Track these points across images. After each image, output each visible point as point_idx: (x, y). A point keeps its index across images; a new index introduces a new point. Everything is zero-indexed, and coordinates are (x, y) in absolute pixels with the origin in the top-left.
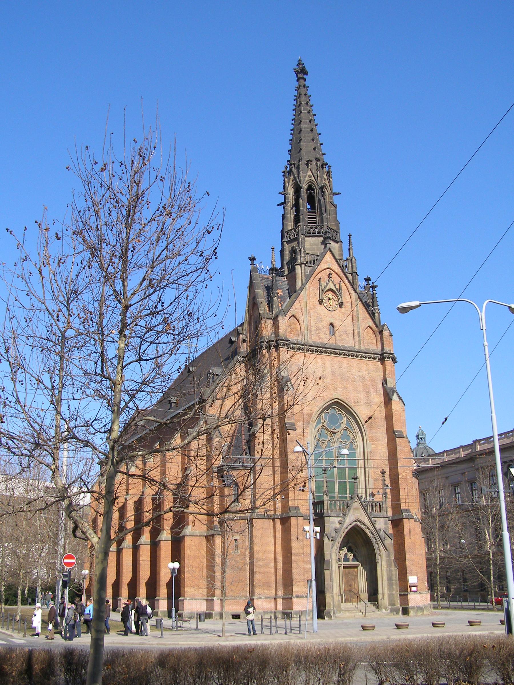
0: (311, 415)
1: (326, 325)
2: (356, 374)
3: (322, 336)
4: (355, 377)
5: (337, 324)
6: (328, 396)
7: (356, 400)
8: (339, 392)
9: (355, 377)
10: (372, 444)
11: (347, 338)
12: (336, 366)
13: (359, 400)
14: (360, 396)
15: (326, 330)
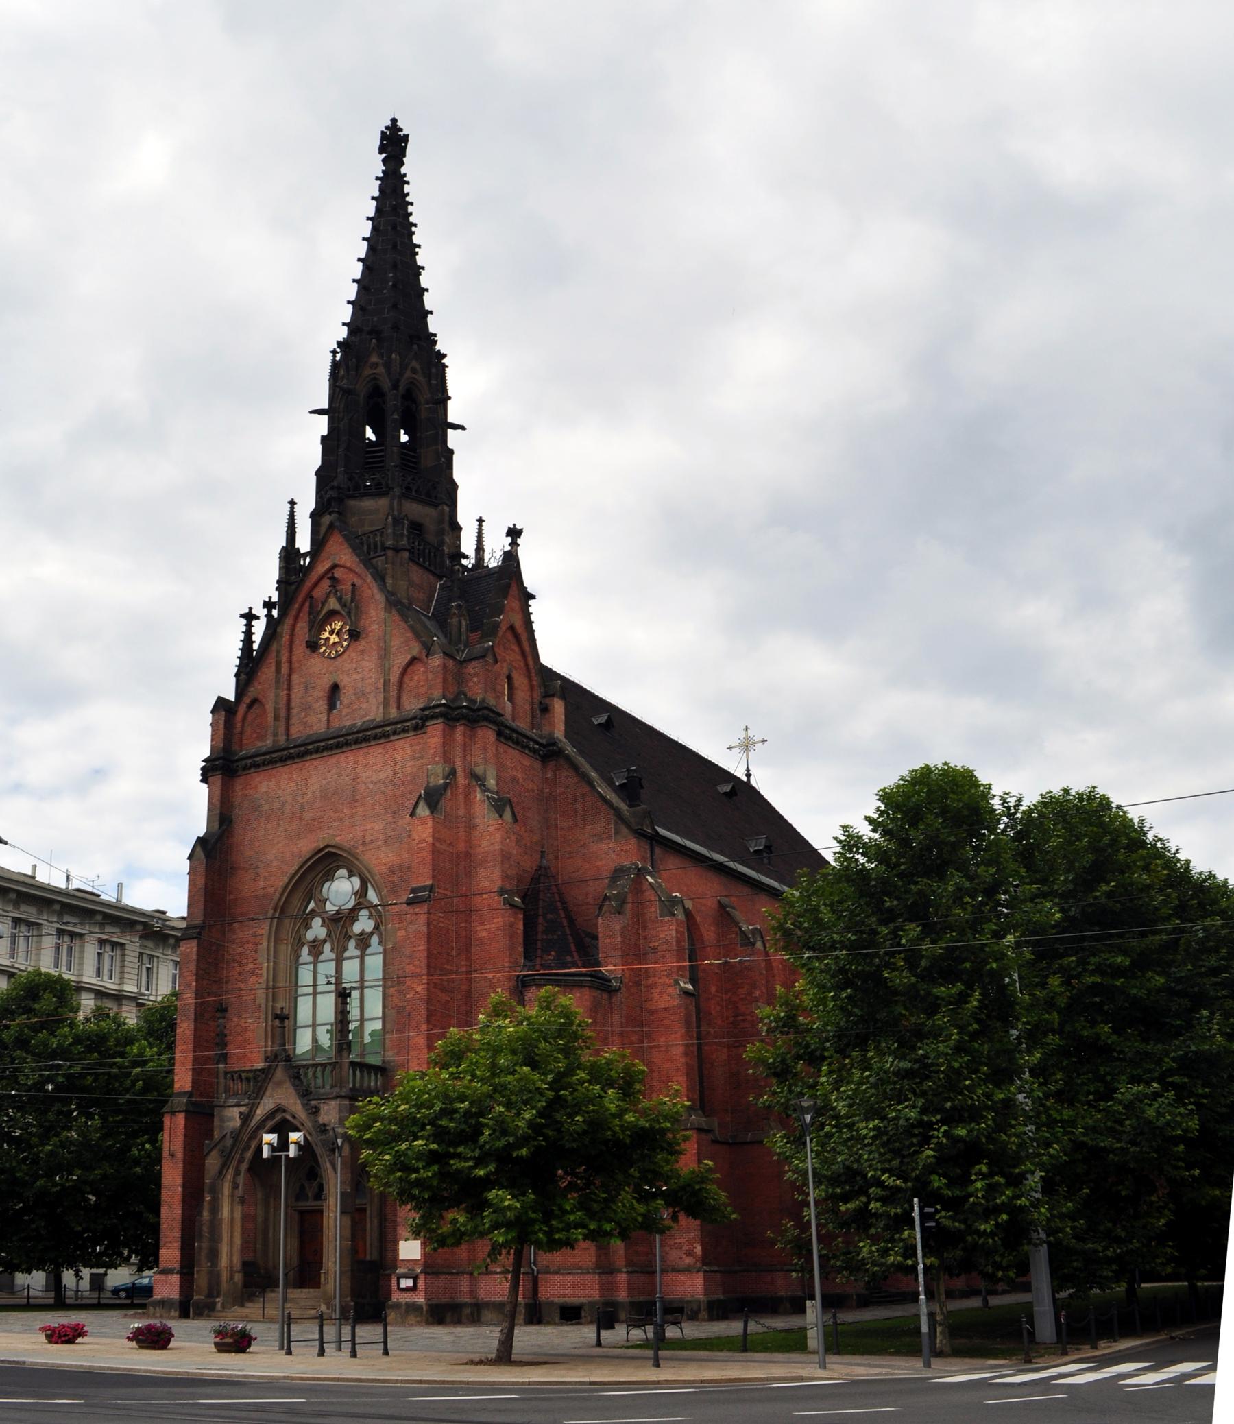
0: (273, 894)
1: (321, 694)
2: (374, 779)
3: (312, 719)
4: (371, 786)
5: (344, 681)
6: (306, 847)
7: (368, 839)
8: (331, 832)
9: (371, 786)
10: (399, 929)
11: (364, 706)
12: (329, 775)
13: (376, 836)
14: (377, 827)
15: (322, 705)
